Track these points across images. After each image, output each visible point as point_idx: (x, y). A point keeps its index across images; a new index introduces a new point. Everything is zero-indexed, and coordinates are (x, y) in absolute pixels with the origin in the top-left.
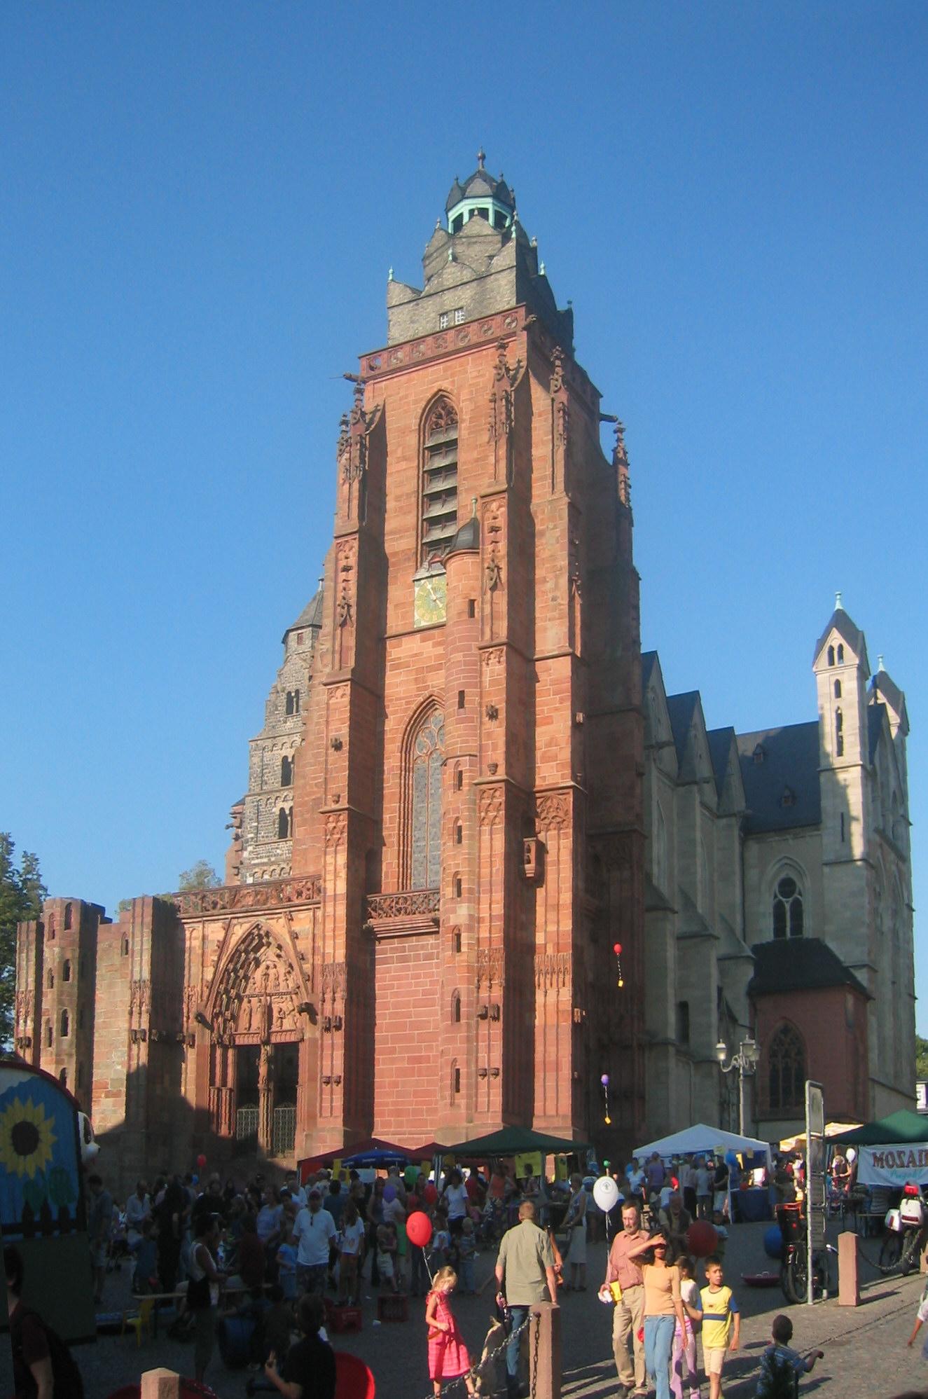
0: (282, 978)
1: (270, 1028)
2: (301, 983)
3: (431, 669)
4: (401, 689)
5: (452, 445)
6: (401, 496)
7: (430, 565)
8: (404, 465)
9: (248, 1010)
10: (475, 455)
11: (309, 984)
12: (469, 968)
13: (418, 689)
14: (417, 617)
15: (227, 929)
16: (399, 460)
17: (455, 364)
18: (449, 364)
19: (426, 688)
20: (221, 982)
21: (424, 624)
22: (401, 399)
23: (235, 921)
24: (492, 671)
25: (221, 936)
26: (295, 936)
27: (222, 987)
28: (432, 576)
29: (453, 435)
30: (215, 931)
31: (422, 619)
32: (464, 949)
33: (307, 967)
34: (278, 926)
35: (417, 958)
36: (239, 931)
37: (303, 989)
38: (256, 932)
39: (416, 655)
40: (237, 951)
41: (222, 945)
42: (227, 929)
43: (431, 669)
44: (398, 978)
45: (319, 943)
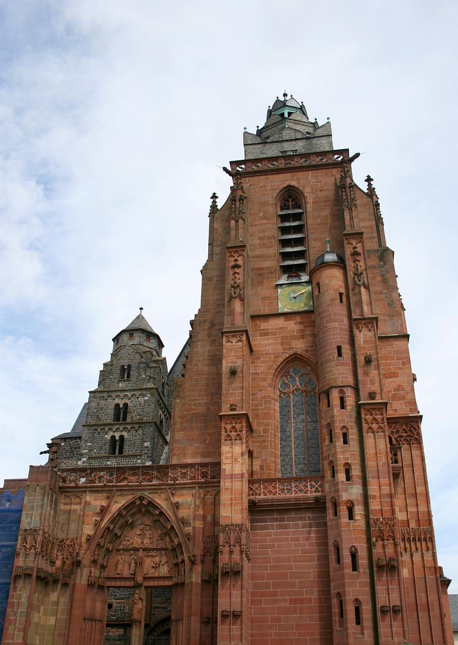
3: (293, 338)
10: (319, 221)
13: (284, 349)
16: (261, 218)
17: (300, 175)
18: (295, 173)
20: (102, 537)
21: (286, 310)
22: (261, 187)
24: (365, 335)
25: (104, 503)
28: (292, 284)
33: (188, 529)
34: (160, 500)
39: (281, 328)
40: (119, 514)
43: (293, 338)
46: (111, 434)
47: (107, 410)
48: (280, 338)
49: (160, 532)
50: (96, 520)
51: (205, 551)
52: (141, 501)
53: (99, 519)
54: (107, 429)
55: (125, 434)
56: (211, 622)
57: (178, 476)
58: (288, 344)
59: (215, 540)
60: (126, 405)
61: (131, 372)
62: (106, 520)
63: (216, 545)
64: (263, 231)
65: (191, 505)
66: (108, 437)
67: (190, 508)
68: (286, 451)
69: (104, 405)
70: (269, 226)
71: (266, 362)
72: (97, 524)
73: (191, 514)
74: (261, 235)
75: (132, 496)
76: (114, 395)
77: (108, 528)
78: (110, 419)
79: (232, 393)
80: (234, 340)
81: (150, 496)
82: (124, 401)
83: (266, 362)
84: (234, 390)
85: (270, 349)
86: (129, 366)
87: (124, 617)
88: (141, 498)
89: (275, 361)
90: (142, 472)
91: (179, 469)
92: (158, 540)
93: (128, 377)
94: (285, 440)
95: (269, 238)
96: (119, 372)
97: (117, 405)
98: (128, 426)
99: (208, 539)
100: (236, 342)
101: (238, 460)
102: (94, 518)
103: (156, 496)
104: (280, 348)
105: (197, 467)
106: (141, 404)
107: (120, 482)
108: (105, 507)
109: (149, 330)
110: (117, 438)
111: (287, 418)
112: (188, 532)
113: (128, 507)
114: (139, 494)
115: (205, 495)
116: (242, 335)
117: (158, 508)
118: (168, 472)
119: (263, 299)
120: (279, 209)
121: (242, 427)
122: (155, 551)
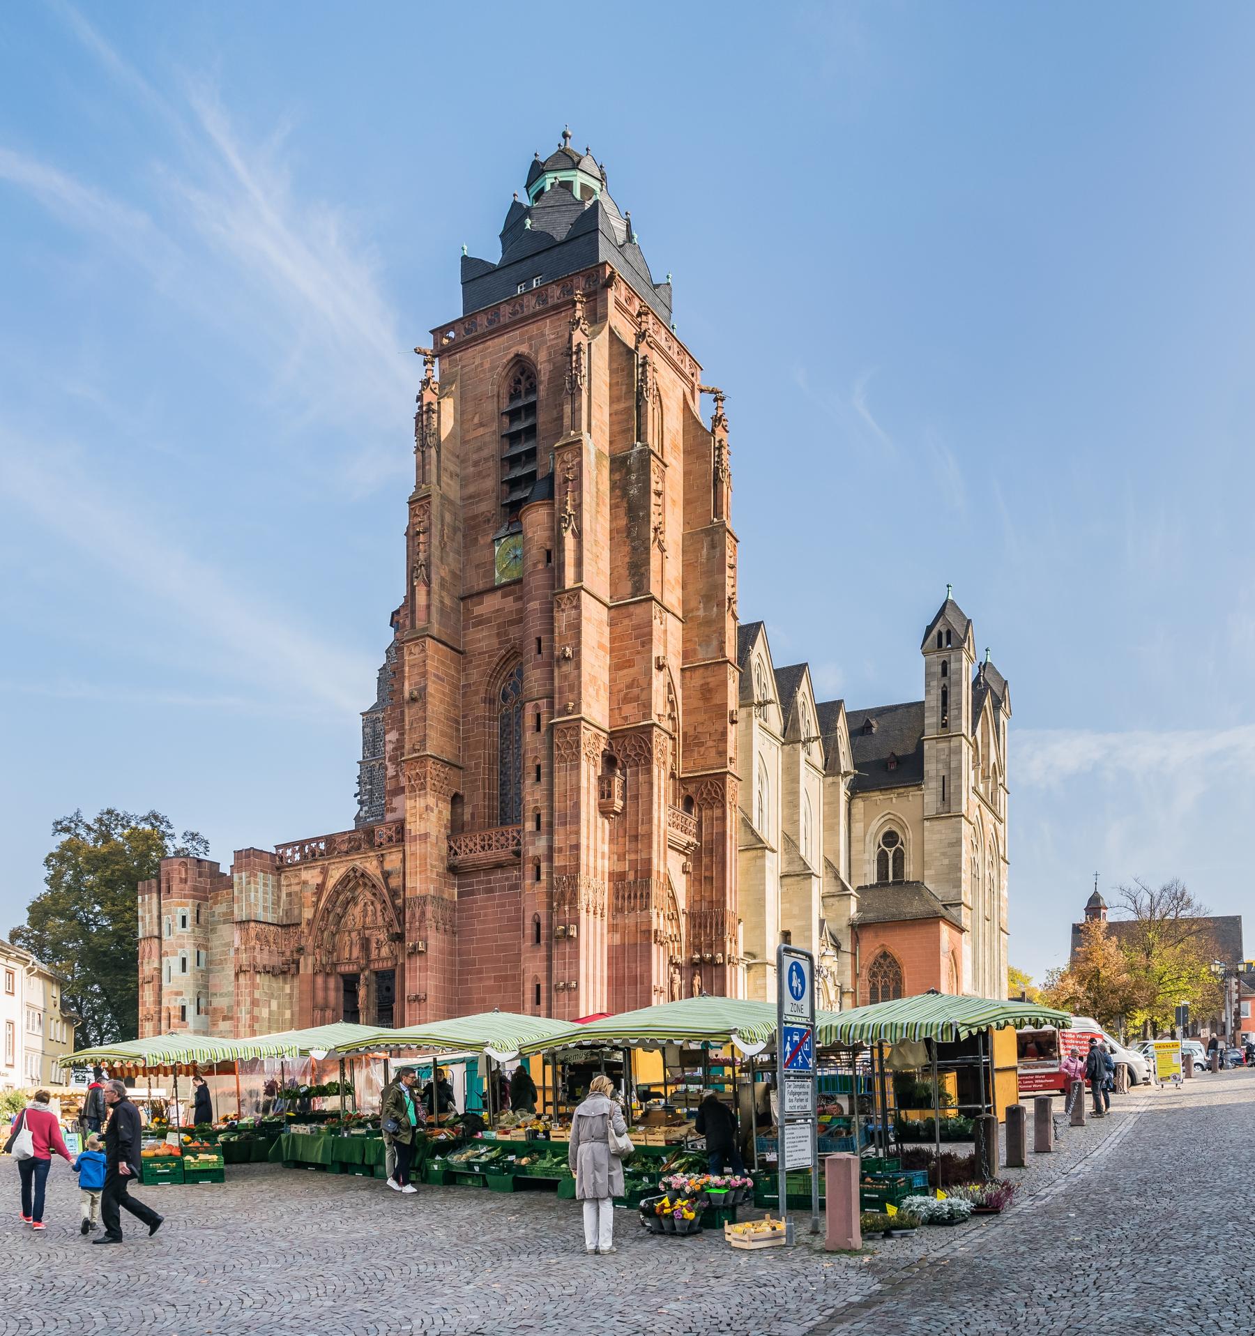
4: (483, 644)
5: (531, 409)
6: (479, 461)
7: (510, 524)
8: (481, 431)
12: (550, 895)
14: (497, 575)
15: (325, 872)
19: (508, 641)
25: (319, 880)
29: (532, 399)
31: (499, 578)
32: (543, 877)
35: (502, 888)
36: (337, 873)
38: (352, 874)
39: (498, 611)
42: (325, 872)
44: (485, 907)
62: (323, 900)
64: (480, 449)
70: (487, 439)
71: (479, 666)
74: (475, 457)
77: (327, 911)
83: (479, 666)
85: (483, 645)
89: (489, 663)
95: (486, 460)
103: (368, 865)
113: (345, 880)
114: (351, 865)
119: (477, 566)
120: (506, 401)
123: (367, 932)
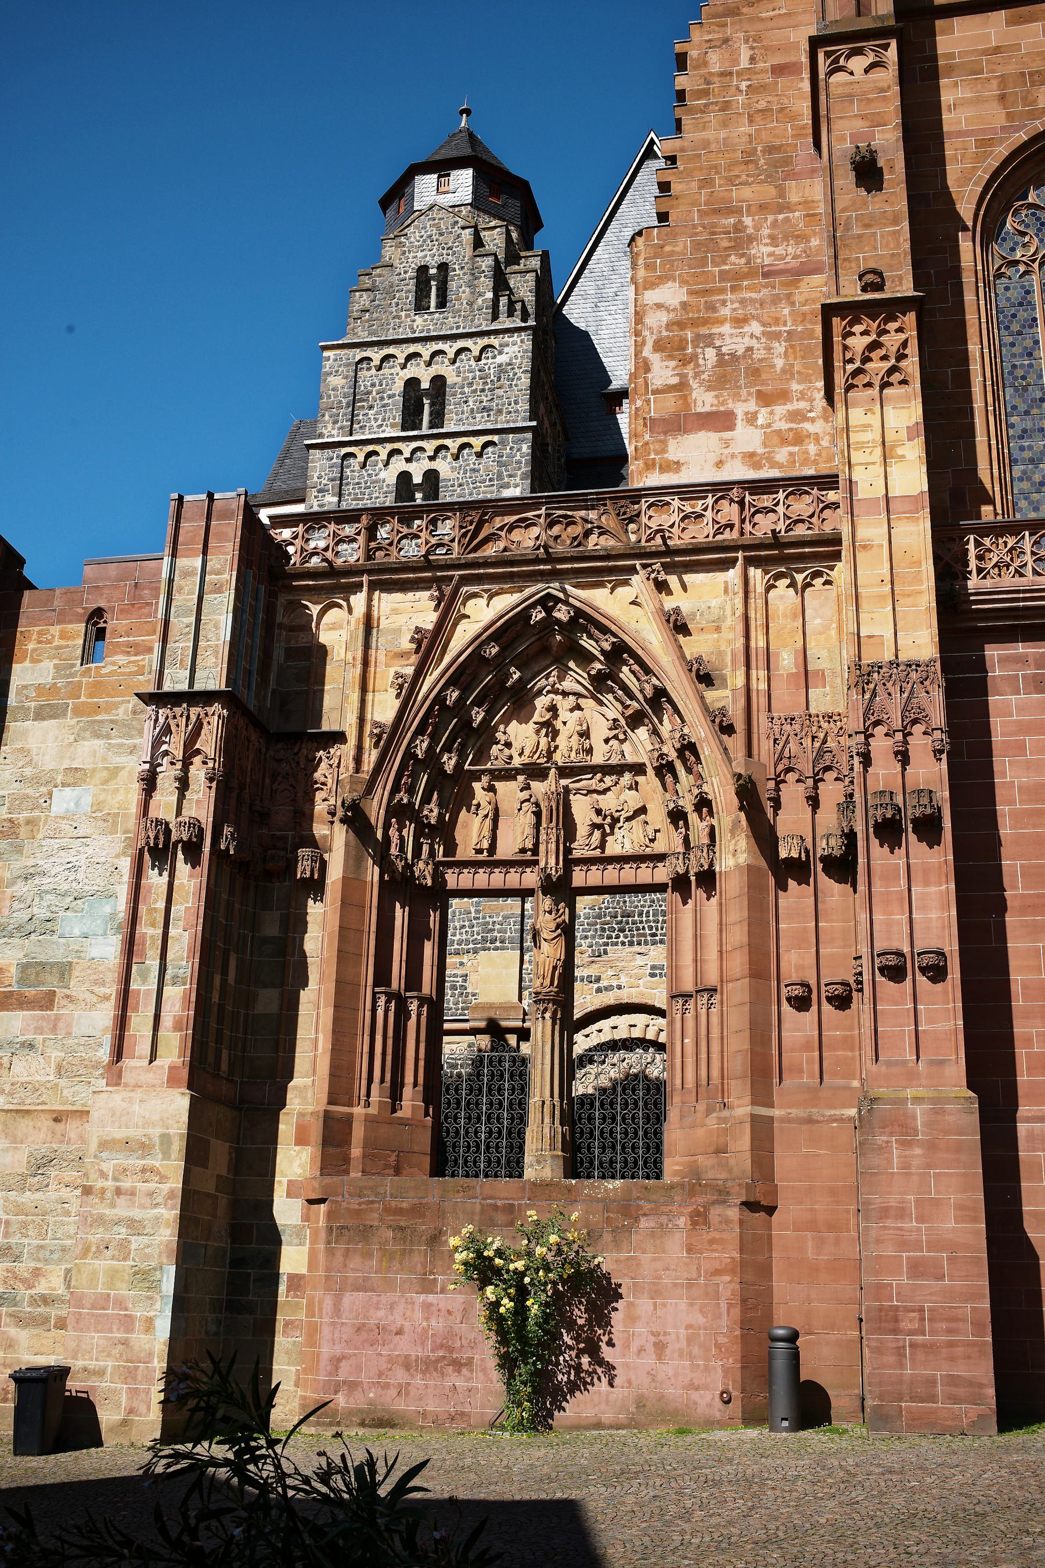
0: (600, 730)
1: (568, 851)
2: (700, 731)
9: (486, 809)
11: (736, 743)
13: (1009, 116)
20: (420, 731)
23: (475, 589)
25: (428, 619)
26: (679, 627)
27: (422, 747)
30: (409, 612)
36: (483, 611)
37: (708, 750)
41: (429, 644)
45: (758, 641)
46: (399, 465)
47: (382, 399)
48: (995, 83)
49: (612, 714)
50: (398, 676)
51: (780, 767)
52: (549, 611)
53: (410, 671)
54: (384, 451)
55: (443, 466)
56: (814, 996)
57: (672, 526)
58: (1024, 99)
59: (814, 729)
60: (439, 381)
61: (453, 285)
63: (817, 745)
65: (721, 619)
66: (390, 476)
67: (718, 629)
68: (1030, 448)
69: (373, 385)
72: (407, 691)
73: (723, 648)
75: (516, 598)
76: (400, 353)
78: (393, 426)
79: (860, 236)
80: (858, 64)
81: (582, 593)
82: (434, 370)
84: (867, 226)
86: (443, 267)
87: (463, 1009)
88: (547, 602)
89: (979, 158)
90: (548, 515)
91: (676, 503)
92: (607, 741)
93: (442, 303)
94: (1027, 413)
96: (412, 285)
97: (412, 384)
98: (448, 442)
99: (787, 727)
100: (866, 71)
101: (900, 451)
102: (392, 672)
104: (996, 116)
105: (735, 493)
106: (488, 376)
107: (475, 549)
108: (426, 631)
109: (493, 162)
110: (417, 479)
111: (1029, 343)
112: (720, 705)
113: (509, 631)
115: (769, 588)
116: (886, 47)
117: (605, 630)
118: (638, 515)
121: (905, 344)
122: (599, 775)
123: (564, 782)
